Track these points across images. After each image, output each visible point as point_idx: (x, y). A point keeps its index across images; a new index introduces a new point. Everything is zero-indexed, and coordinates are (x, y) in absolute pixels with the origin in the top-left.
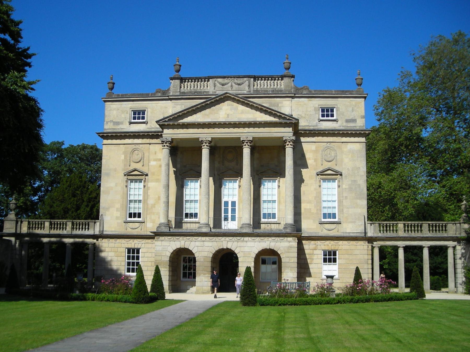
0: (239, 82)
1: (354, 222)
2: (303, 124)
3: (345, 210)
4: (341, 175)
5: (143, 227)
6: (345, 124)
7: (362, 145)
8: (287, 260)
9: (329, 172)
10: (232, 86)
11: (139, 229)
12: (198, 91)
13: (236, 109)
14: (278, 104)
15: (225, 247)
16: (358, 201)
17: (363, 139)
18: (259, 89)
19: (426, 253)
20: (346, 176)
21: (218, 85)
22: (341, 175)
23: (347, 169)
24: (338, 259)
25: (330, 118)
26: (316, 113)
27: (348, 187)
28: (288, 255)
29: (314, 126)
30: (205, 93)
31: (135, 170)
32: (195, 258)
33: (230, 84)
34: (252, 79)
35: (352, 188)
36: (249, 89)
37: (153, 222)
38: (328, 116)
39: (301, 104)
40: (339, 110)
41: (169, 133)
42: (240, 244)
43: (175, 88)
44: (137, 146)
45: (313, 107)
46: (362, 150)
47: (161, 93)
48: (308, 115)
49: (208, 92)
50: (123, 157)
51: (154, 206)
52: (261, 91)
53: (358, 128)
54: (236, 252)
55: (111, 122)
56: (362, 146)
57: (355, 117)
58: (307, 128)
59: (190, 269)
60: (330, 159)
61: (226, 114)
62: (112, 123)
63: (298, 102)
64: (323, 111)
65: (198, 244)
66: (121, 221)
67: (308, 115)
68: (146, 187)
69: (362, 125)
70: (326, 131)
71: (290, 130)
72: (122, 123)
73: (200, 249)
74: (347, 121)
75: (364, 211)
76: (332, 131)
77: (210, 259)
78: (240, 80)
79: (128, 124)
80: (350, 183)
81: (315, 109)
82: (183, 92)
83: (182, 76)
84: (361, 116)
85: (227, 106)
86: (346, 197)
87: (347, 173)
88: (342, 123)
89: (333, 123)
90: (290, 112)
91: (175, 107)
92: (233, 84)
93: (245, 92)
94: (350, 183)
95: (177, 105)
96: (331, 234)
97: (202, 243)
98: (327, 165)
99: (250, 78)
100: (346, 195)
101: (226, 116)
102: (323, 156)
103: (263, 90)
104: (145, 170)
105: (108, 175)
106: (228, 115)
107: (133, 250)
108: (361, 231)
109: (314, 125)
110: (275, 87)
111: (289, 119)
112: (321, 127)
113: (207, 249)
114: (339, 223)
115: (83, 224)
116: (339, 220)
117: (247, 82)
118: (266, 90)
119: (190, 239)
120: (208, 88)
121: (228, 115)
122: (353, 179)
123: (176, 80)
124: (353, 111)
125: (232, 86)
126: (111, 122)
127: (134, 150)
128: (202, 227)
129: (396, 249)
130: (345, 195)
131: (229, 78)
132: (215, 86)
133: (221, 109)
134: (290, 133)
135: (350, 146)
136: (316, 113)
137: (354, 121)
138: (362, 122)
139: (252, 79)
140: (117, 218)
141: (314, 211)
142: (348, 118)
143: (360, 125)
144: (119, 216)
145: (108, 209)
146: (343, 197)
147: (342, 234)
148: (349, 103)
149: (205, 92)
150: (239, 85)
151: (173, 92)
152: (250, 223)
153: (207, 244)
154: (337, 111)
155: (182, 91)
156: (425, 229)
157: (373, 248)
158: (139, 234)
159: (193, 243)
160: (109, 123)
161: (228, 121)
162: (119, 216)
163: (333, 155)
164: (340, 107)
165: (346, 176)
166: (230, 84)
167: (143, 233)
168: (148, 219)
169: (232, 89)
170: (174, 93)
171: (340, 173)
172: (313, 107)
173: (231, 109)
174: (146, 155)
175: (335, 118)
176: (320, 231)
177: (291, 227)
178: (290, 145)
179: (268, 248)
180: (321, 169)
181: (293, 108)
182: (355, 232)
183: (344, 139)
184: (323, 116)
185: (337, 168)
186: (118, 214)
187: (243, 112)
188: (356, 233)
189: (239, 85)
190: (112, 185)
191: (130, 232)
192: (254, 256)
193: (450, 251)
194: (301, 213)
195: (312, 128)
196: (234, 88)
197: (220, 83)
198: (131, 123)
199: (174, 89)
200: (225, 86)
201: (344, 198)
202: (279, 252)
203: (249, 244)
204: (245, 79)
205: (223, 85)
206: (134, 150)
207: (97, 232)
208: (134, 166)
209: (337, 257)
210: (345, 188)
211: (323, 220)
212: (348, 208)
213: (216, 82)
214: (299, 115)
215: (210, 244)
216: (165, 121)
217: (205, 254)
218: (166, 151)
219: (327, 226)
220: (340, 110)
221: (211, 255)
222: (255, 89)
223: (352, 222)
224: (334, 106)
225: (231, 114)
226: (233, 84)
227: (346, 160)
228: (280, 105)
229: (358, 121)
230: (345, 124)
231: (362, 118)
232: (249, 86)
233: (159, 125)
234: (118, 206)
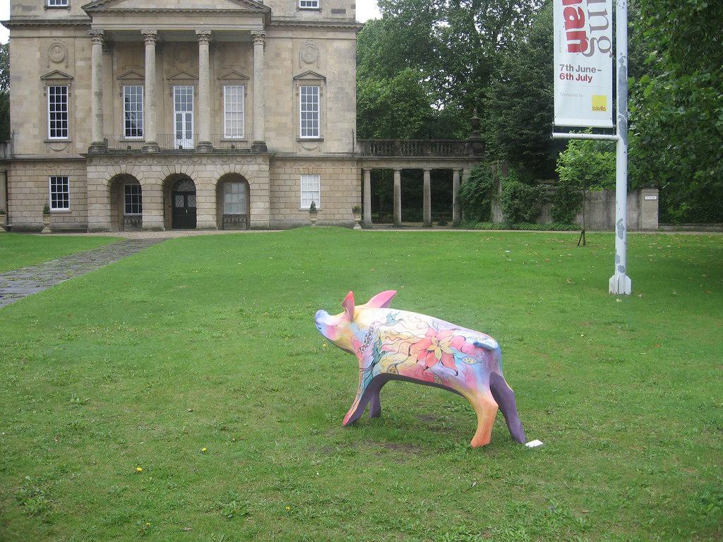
2: (276, 13)
3: (329, 125)
6: (330, 15)
8: (257, 187)
9: (310, 77)
11: (64, 152)
15: (178, 172)
17: (353, 36)
19: (427, 177)
20: (331, 82)
22: (325, 79)
28: (257, 180)
29: (291, 17)
31: (57, 72)
32: (140, 187)
37: (85, 141)
41: (99, 23)
42: (197, 168)
44: (58, 41)
50: (38, 55)
51: (84, 120)
53: (347, 21)
55: (19, 7)
58: (282, 19)
59: (135, 201)
60: (311, 60)
62: (21, 9)
65: (142, 168)
66: (38, 141)
68: (73, 95)
70: (306, 22)
72: (34, 8)
73: (147, 174)
74: (334, 11)
76: (315, 23)
77: (160, 188)
79: (43, 9)
80: (336, 90)
86: (331, 108)
94: (336, 90)
97: (148, 167)
98: (307, 68)
100: (331, 106)
104: (70, 72)
105: (19, 79)
107: (59, 179)
111: (258, 7)
113: (155, 175)
114: (321, 140)
126: (19, 7)
127: (53, 47)
129: (392, 171)
130: (329, 105)
135: (337, 44)
140: (35, 137)
141: (290, 125)
143: (348, 17)
144: (37, 133)
145: (21, 125)
146: (327, 108)
153: (154, 168)
157: (363, 172)
158: (65, 157)
160: (17, 8)
162: (37, 133)
165: (331, 82)
167: (70, 156)
168: (77, 137)
174: (71, 50)
175: (318, 7)
176: (298, 151)
180: (298, 72)
183: (331, 35)
185: (320, 72)
186: (36, 131)
190: (27, 93)
191: (53, 155)
192: (215, 182)
193: (456, 176)
195: (288, 19)
198: (47, 8)
201: (328, 110)
202: (246, 177)
206: (53, 47)
207: (8, 157)
208: (54, 67)
211: (302, 137)
215: (159, 168)
216: (94, 7)
217: (153, 181)
218: (97, 48)
219: (306, 145)
221: (160, 182)
223: (338, 140)
227: (331, 62)
230: (330, 15)
233: (86, 12)
234: (36, 120)
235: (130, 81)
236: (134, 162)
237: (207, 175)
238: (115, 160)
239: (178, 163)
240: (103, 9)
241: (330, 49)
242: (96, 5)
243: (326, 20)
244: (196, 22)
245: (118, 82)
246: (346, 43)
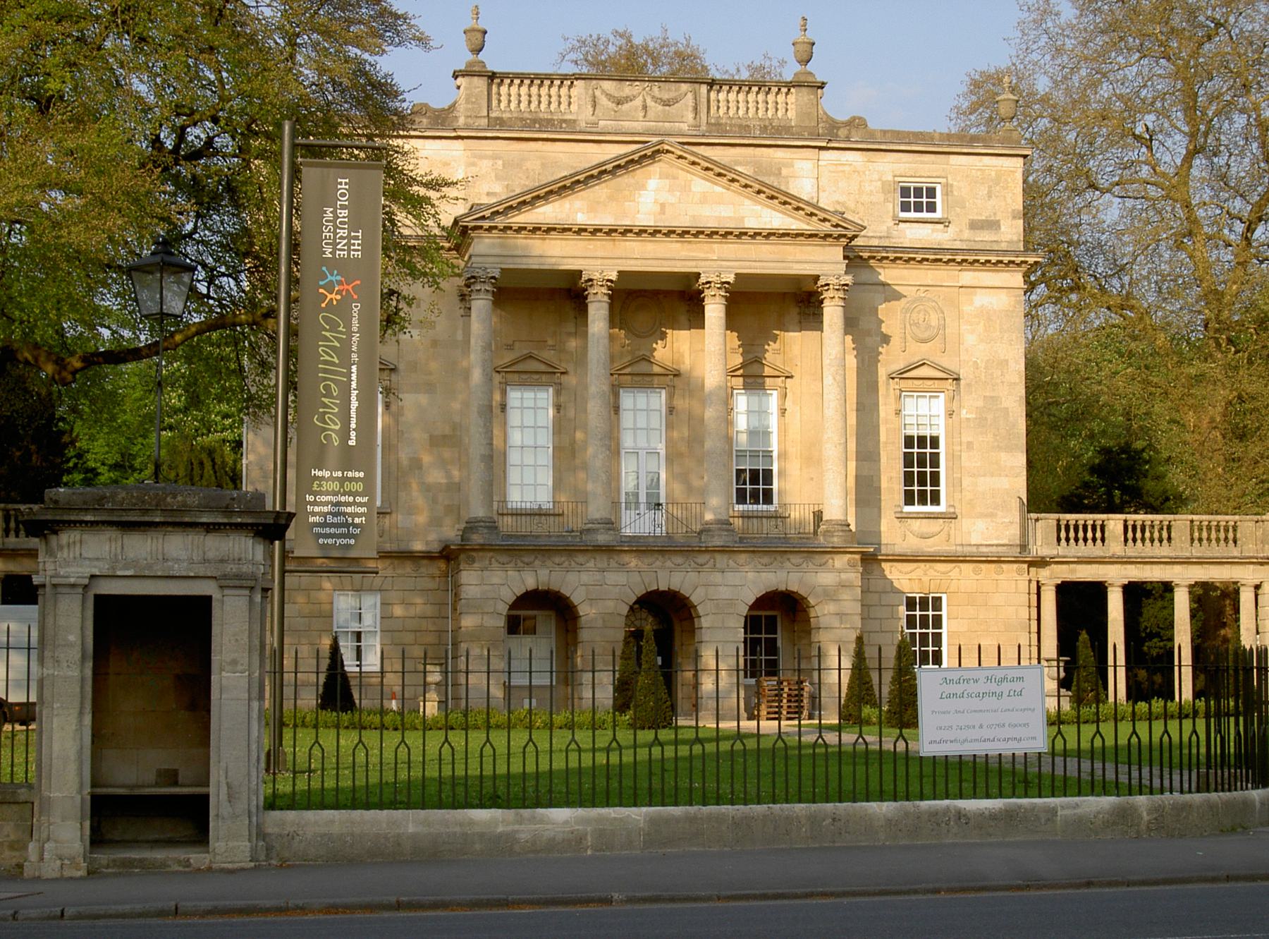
0: (666, 96)
1: (992, 515)
3: (966, 482)
4: (957, 379)
5: (952, 532)
6: (967, 234)
7: (1016, 296)
10: (645, 107)
12: (541, 115)
13: (686, 188)
14: (780, 169)
15: (663, 587)
16: (1003, 455)
18: (724, 121)
19: (1182, 604)
21: (603, 101)
22: (957, 379)
23: (971, 363)
24: (948, 619)
25: (925, 215)
26: (886, 200)
27: (974, 416)
29: (881, 237)
30: (564, 125)
33: (638, 102)
34: (704, 88)
35: (986, 419)
36: (695, 118)
38: (918, 208)
39: (844, 171)
40: (952, 192)
43: (473, 103)
45: (880, 180)
46: (1013, 311)
47: (429, 117)
48: (863, 204)
49: (575, 121)
52: (730, 125)
53: (1004, 246)
54: (694, 599)
56: (1013, 299)
57: (995, 214)
60: (926, 335)
61: (656, 202)
63: (836, 165)
64: (905, 192)
65: (585, 577)
67: (863, 204)
69: (1015, 238)
71: (837, 253)
74: (974, 225)
75: (1018, 484)
78: (669, 90)
80: (980, 403)
81: (885, 186)
82: (497, 118)
83: (492, 67)
84: (1013, 210)
85: (660, 178)
86: (970, 445)
87: (971, 377)
88: (961, 231)
89: (933, 231)
90: (815, 195)
91: (474, 164)
92: (650, 102)
93: (684, 127)
94: (980, 403)
95: (482, 157)
96: (929, 550)
97: (598, 576)
99: (697, 86)
100: (970, 439)
101: (658, 208)
102: (908, 326)
103: (735, 125)
106: (663, 206)
108: (1009, 540)
109: (882, 235)
110: (770, 114)
111: (837, 226)
112: (902, 240)
115: (1209, 528)
116: (952, 510)
117: (690, 96)
118: (745, 123)
119: (564, 565)
120: (574, 108)
121: (663, 206)
122: (988, 394)
123: (476, 78)
124: (990, 197)
125: (645, 107)
128: (598, 530)
131: (637, 83)
132: (594, 106)
133: (643, 187)
134: (839, 266)
135: (982, 300)
136: (886, 200)
137: (993, 225)
138: (1014, 230)
139: (704, 88)
142: (976, 218)
143: (1008, 237)
147: (959, 549)
148: (979, 173)
149: (565, 121)
150: (667, 103)
151: (467, 117)
152: (842, 518)
154: (946, 194)
155: (493, 115)
156: (1180, 537)
159: (572, 578)
161: (667, 224)
163: (934, 323)
164: (955, 183)
165: (969, 385)
166: (638, 102)
169: (645, 116)
170: (470, 121)
171: (955, 376)
172: (880, 180)
173: (671, 190)
175: (938, 215)
177: (842, 531)
178: (837, 299)
179: (782, 588)
181: (823, 181)
182: (995, 542)
183: (968, 277)
184: (905, 207)
185: (945, 362)
187: (704, 200)
188: (997, 545)
189: (667, 103)
193: (1246, 597)
194: (880, 488)
196: (651, 114)
197: (609, 96)
199: (470, 106)
200: (625, 107)
201: (964, 447)
203: (731, 578)
204: (684, 87)
205: (619, 102)
209: (944, 613)
210: (967, 419)
212: (973, 475)
213: (598, 93)
214: (839, 203)
216: (483, 218)
219: (916, 524)
220: (955, 193)
222: (713, 121)
223: (982, 516)
224: (938, 180)
225: (672, 204)
226: (650, 102)
227: (970, 339)
228: (784, 172)
229: (1003, 228)
230: (967, 234)
231: (1014, 218)
232: (696, 109)
235: (524, 376)
236: (804, 565)
237: (724, 593)
238: (526, 560)
239: (662, 568)
240: (500, 221)
241: (966, 308)
242: (487, 213)
243: (958, 245)
244: (702, 255)
245: (497, 378)
246: (1003, 294)
